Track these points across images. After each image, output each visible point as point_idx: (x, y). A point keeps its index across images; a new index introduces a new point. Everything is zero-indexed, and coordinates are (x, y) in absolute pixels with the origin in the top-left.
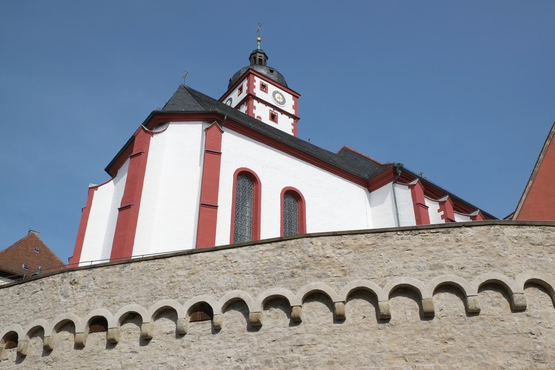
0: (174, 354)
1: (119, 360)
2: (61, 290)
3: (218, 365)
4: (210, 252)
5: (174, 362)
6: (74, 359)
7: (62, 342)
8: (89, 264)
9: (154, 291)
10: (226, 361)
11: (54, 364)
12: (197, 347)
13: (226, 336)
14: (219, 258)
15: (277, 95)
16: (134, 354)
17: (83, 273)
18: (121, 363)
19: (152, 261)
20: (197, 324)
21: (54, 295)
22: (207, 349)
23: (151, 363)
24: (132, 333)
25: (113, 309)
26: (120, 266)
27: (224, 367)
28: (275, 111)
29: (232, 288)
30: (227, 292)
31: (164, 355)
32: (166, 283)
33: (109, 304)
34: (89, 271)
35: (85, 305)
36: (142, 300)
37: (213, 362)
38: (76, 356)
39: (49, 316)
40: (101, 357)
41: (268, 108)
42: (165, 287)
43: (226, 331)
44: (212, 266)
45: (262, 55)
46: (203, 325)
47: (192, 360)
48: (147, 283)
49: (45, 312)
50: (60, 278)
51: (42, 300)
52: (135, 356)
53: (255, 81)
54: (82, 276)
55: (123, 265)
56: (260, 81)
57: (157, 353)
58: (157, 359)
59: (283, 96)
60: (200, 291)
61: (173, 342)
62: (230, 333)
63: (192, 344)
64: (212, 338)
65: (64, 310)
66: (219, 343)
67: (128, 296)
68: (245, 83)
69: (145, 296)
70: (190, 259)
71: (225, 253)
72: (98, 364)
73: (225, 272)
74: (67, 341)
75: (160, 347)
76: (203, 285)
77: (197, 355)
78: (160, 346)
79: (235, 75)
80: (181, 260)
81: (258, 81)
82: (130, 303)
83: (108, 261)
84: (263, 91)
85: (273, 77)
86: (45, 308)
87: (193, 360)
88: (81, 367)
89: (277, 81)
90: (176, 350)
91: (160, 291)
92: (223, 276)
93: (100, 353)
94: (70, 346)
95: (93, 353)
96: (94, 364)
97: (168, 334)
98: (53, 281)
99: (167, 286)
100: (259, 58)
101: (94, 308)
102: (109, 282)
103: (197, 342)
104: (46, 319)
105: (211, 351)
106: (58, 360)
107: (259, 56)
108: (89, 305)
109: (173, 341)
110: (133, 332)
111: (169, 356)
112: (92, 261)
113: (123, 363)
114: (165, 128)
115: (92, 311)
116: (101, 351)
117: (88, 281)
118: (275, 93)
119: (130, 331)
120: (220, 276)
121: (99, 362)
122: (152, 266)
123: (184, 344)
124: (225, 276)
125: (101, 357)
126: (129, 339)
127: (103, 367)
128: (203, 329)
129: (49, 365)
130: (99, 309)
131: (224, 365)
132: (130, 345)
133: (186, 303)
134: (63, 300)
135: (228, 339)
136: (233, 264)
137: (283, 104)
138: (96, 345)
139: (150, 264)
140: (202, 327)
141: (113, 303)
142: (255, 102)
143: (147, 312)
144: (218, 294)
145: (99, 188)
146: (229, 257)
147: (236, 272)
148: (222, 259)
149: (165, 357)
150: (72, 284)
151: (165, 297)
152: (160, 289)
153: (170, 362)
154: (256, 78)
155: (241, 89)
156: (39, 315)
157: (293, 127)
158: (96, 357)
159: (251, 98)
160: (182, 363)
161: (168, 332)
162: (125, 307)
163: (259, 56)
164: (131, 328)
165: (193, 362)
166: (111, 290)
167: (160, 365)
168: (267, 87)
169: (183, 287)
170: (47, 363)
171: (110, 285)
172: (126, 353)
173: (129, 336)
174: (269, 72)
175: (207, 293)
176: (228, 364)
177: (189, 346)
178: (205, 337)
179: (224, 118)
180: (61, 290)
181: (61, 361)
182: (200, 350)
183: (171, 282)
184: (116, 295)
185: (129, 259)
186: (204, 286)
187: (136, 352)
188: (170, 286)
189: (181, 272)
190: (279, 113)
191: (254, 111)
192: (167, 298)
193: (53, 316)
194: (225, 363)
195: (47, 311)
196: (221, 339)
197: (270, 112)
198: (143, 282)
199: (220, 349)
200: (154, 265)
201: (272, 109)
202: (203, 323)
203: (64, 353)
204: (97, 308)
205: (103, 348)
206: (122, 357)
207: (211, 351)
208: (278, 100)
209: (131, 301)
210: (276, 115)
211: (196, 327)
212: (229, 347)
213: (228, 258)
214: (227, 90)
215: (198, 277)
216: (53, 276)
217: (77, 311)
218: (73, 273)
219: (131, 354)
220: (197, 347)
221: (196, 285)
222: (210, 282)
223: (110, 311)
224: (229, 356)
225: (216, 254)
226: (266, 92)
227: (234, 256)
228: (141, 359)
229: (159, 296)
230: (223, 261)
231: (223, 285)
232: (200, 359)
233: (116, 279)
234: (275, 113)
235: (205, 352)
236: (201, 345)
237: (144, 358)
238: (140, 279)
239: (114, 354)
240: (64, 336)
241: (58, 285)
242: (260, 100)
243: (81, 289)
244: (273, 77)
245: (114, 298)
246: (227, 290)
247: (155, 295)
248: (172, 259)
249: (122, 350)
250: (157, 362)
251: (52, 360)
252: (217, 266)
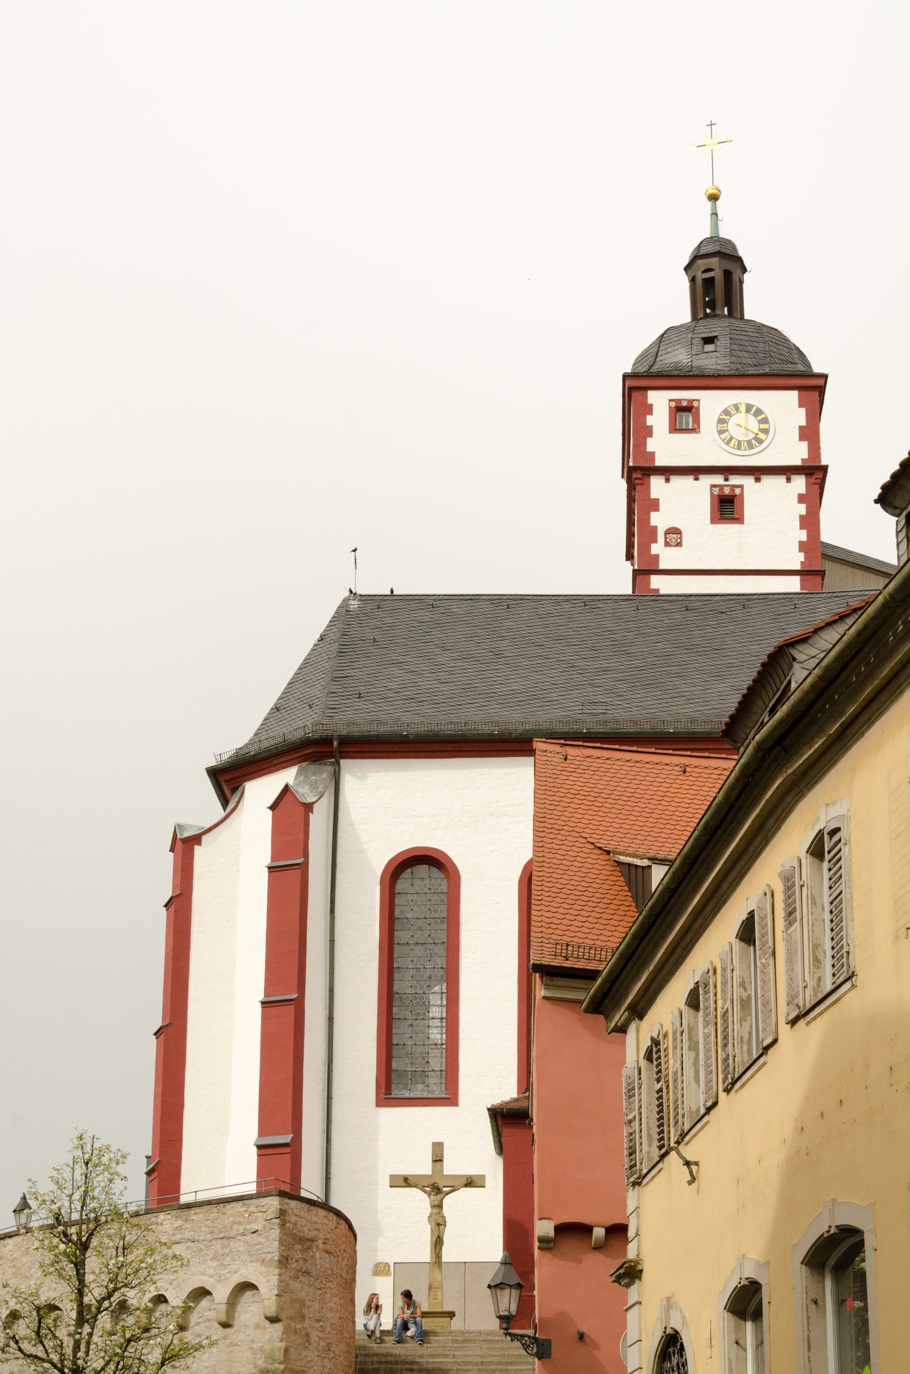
28: (735, 480)
41: (707, 481)
45: (714, 262)
53: (649, 409)
56: (670, 400)
59: (759, 412)
85: (713, 361)
89: (733, 366)
137: (761, 442)
142: (657, 484)
157: (802, 509)
159: (640, 479)
168: (698, 409)
190: (747, 482)
191: (655, 519)
197: (712, 494)
201: (719, 480)
210: (737, 491)
234: (733, 487)
242: (668, 472)
244: (713, 361)
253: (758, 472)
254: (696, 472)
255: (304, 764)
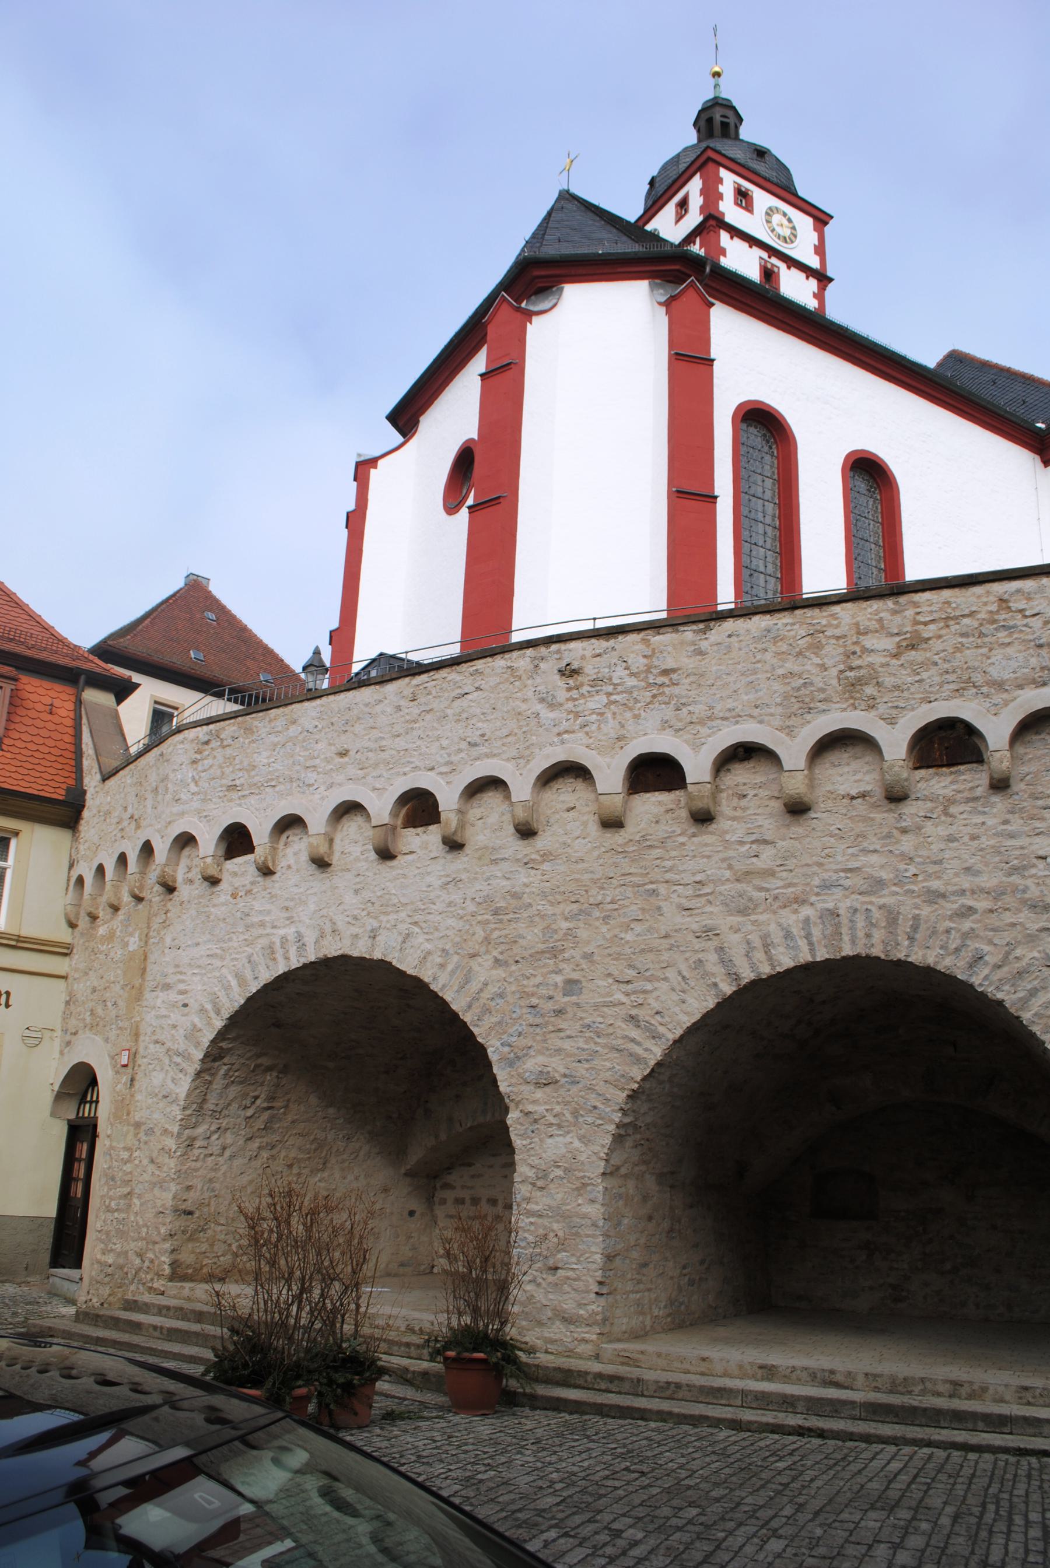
0: (878, 847)
1: (723, 860)
2: (538, 689)
3: (1010, 875)
4: (957, 590)
5: (882, 867)
6: (599, 857)
7: (558, 816)
8: (588, 626)
9: (803, 691)
10: (1034, 866)
11: (546, 866)
12: (942, 831)
13: (1025, 804)
14: (985, 604)
15: (776, 218)
16: (762, 847)
17: (592, 647)
18: (730, 867)
19: (786, 613)
20: (937, 774)
21: (518, 703)
22: (974, 838)
23: (815, 868)
24: (749, 797)
25: (692, 736)
26: (694, 627)
27: (1031, 880)
28: (774, 261)
29: (1034, 682)
30: (1020, 692)
31: (850, 851)
32: (834, 672)
33: (680, 725)
34: (607, 641)
35: (610, 726)
36: (772, 715)
37: (995, 867)
38: (603, 849)
39: (514, 753)
40: (674, 853)
41: (757, 253)
42: (835, 682)
43: (1025, 791)
44: (968, 626)
46: (953, 776)
47: (935, 863)
48: (780, 672)
49: (499, 743)
50: (528, 660)
51: (483, 714)
52: (767, 852)
53: (720, 181)
54: (588, 653)
55: (701, 626)
57: (828, 845)
58: (831, 859)
59: (790, 221)
60: (938, 691)
61: (872, 819)
62: (1037, 798)
63: (929, 823)
64: (986, 809)
65: (556, 740)
66: (1006, 822)
67: (730, 704)
68: (695, 186)
69: (777, 704)
70: (897, 607)
71: (1001, 592)
72: (670, 870)
73: (1007, 640)
74: (571, 814)
75: (837, 832)
76: (947, 676)
77: (947, 852)
78: (834, 827)
79: (664, 168)
80: (869, 610)
81: (729, 181)
82: (737, 722)
83: (664, 615)
84: (740, 206)
86: (498, 733)
87: (940, 862)
88: (623, 875)
90: (883, 838)
91: (822, 690)
92: (1002, 651)
93: (669, 844)
94: (585, 824)
95: (648, 843)
96: (656, 869)
97: (853, 798)
98: (509, 667)
99: (839, 679)
100: (722, 123)
101: (636, 733)
102: (668, 667)
103: (943, 818)
104: (508, 760)
105: (985, 842)
106: (556, 857)
107: (722, 116)
108: (623, 726)
109: (872, 815)
110: (752, 793)
111: (866, 851)
112: (595, 619)
113: (736, 868)
114: (554, 301)
115: (635, 742)
116: (669, 837)
117: (610, 667)
118: (770, 212)
119: (743, 789)
120: (994, 652)
121: (668, 864)
122: (789, 628)
123: (904, 824)
124: (1009, 650)
125: (674, 853)
126: (744, 809)
127: (683, 875)
128: (954, 787)
129: (532, 868)
130: (653, 736)
131: (1031, 876)
132: (749, 826)
133: (901, 721)
134: (547, 715)
135: (1031, 812)
136: (1028, 620)
138: (653, 825)
139: (781, 622)
140: (951, 783)
141: (688, 720)
142: (724, 236)
143: (790, 743)
144: (994, 697)
145: (380, 463)
146: (1015, 602)
147: (1041, 641)
148: (994, 608)
149: (853, 855)
150: (564, 675)
151: (838, 706)
152: (821, 685)
153: (872, 866)
154: (723, 173)
155: (683, 204)
156: (482, 750)
158: (656, 852)
160: (906, 870)
161: (853, 792)
162: (726, 730)
163: (722, 116)
164: (745, 784)
165: (936, 868)
166: (676, 690)
167: (842, 874)
168: (752, 197)
169: (887, 679)
170: (526, 864)
171: (674, 676)
172: (741, 843)
173: (744, 803)
174: (755, 156)
175: (962, 695)
176: (1041, 873)
177: (920, 828)
178: (961, 808)
179: (704, 271)
180: (538, 689)
181: (565, 859)
182: (951, 839)
183: (851, 669)
184: (695, 702)
185: (712, 609)
186: (951, 677)
187: (766, 842)
188: (847, 678)
189: (875, 641)
190: (782, 266)
192: (844, 710)
193: (527, 752)
194: (1033, 871)
195: (505, 740)
196: (1013, 813)
198: (768, 667)
199: (1012, 836)
200: (793, 624)
201: (765, 255)
202: (952, 773)
203: (569, 841)
204: (645, 734)
205: (674, 832)
206: (731, 853)
207: (985, 842)
208: (779, 230)
209: (740, 716)
210: (776, 270)
211: (933, 782)
212: (1037, 831)
213: (1011, 604)
214: (641, 212)
215: (928, 655)
216: (507, 656)
217: (591, 740)
218: (562, 646)
219: (754, 846)
220: (942, 831)
221: (925, 675)
222: (965, 666)
223: (686, 741)
224: (1041, 853)
225: (974, 594)
226: (749, 208)
227: (1029, 599)
228: (785, 858)
229: (819, 704)
230: (998, 611)
231: (1006, 675)
232: (956, 862)
233: (688, 663)
234: (773, 265)
235: (970, 843)
236: (954, 827)
237: (795, 857)
238: (759, 662)
239: (706, 845)
240: (563, 802)
241: (524, 677)
242: (735, 232)
243: (592, 686)
245: (690, 708)
246: (1021, 687)
247: (807, 700)
248: (843, 609)
249: (728, 837)
250: (834, 867)
251: (538, 858)
252: (981, 625)
253: (792, 263)
254: (752, 241)
255: (658, 281)
